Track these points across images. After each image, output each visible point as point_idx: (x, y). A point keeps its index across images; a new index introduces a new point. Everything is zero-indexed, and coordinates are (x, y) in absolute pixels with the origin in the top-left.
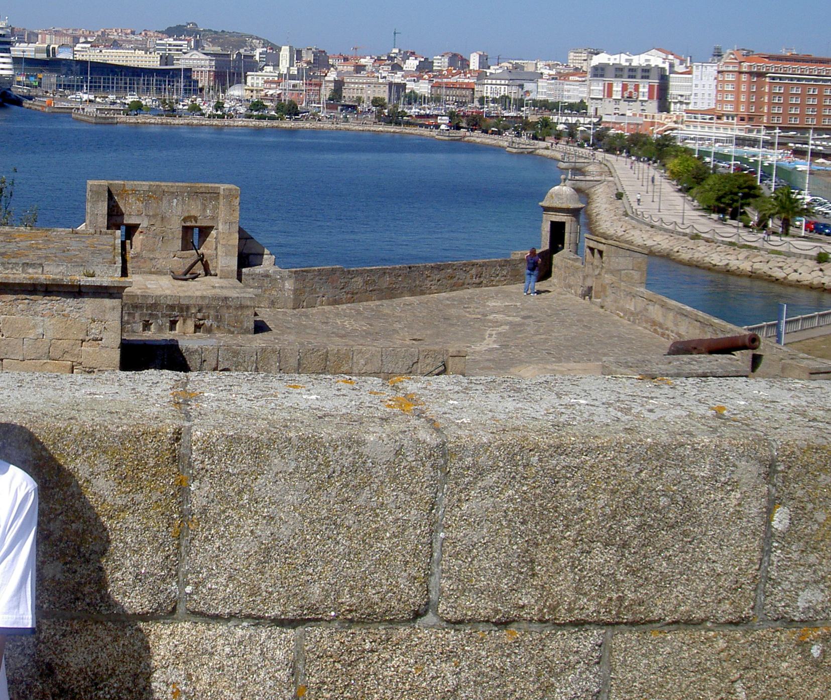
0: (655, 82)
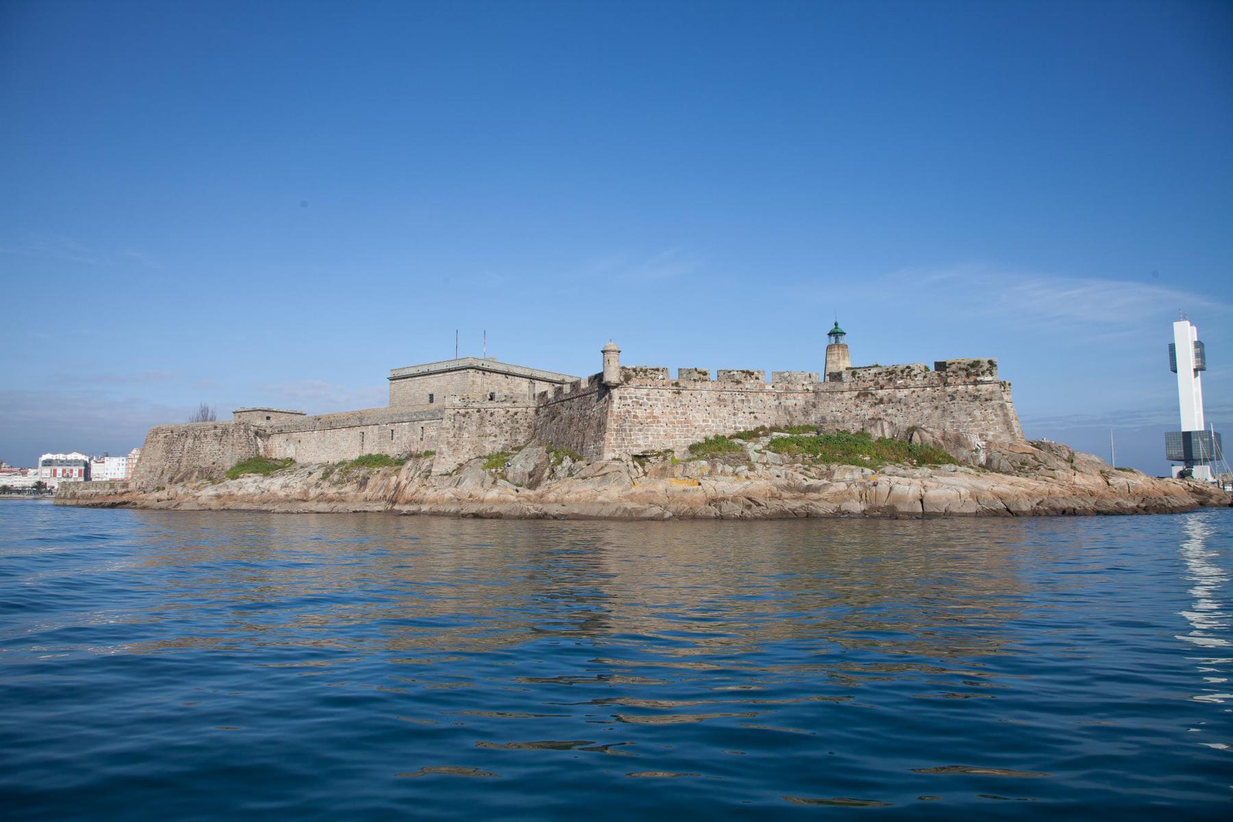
0: (83, 468)
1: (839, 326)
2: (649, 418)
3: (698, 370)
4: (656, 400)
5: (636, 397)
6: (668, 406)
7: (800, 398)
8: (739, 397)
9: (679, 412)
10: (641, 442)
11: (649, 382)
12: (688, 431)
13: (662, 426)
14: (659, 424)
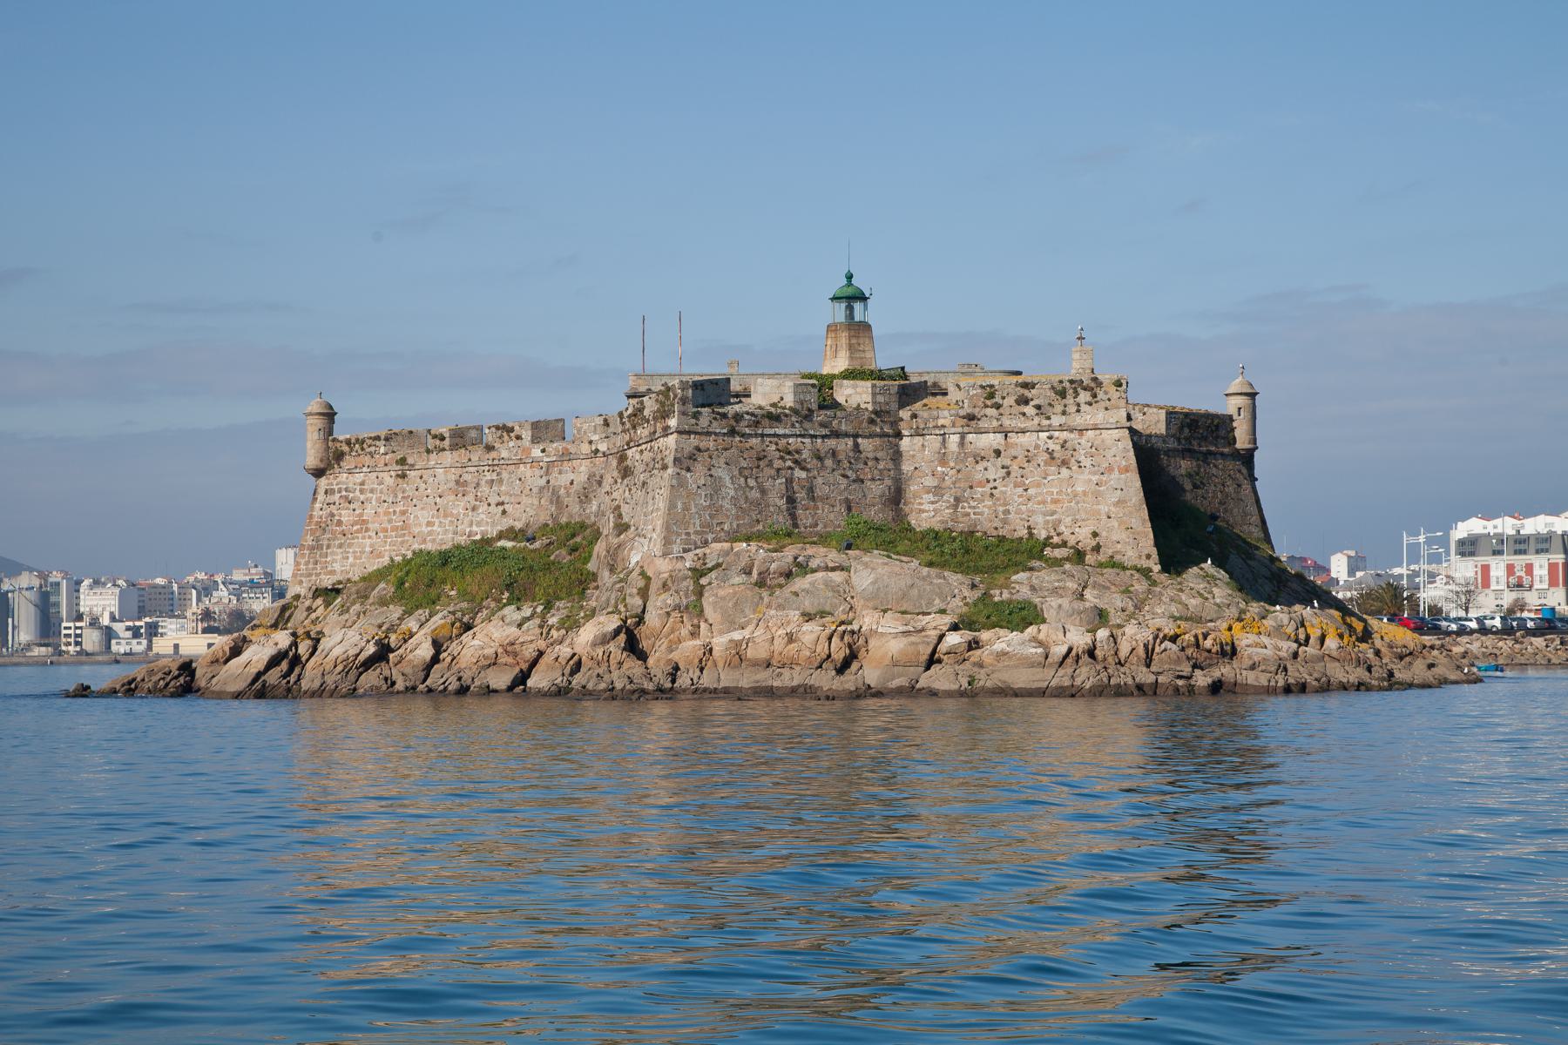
2: (355, 523)
3: (432, 432)
4: (372, 491)
5: (346, 490)
6: (385, 501)
7: (583, 468)
8: (489, 476)
9: (398, 510)
10: (337, 567)
11: (367, 460)
12: (402, 542)
13: (370, 537)
14: (367, 534)
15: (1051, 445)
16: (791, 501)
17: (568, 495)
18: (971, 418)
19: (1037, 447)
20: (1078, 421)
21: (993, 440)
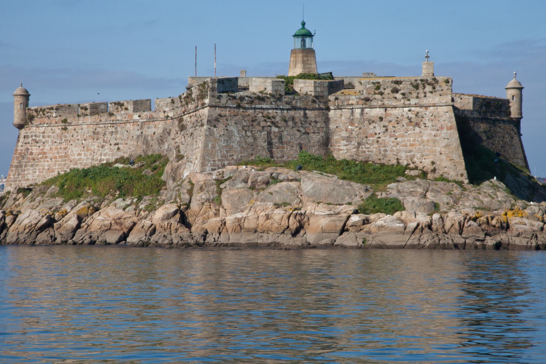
1: (306, 26)
2: (40, 154)
3: (81, 106)
4: (49, 137)
5: (35, 136)
6: (55, 142)
7: (160, 126)
8: (111, 129)
9: (62, 147)
10: (30, 177)
11: (46, 120)
12: (65, 164)
13: (48, 161)
14: (46, 160)
15: (410, 115)
16: (270, 144)
17: (152, 140)
18: (367, 100)
19: (402, 116)
20: (425, 101)
21: (378, 112)
